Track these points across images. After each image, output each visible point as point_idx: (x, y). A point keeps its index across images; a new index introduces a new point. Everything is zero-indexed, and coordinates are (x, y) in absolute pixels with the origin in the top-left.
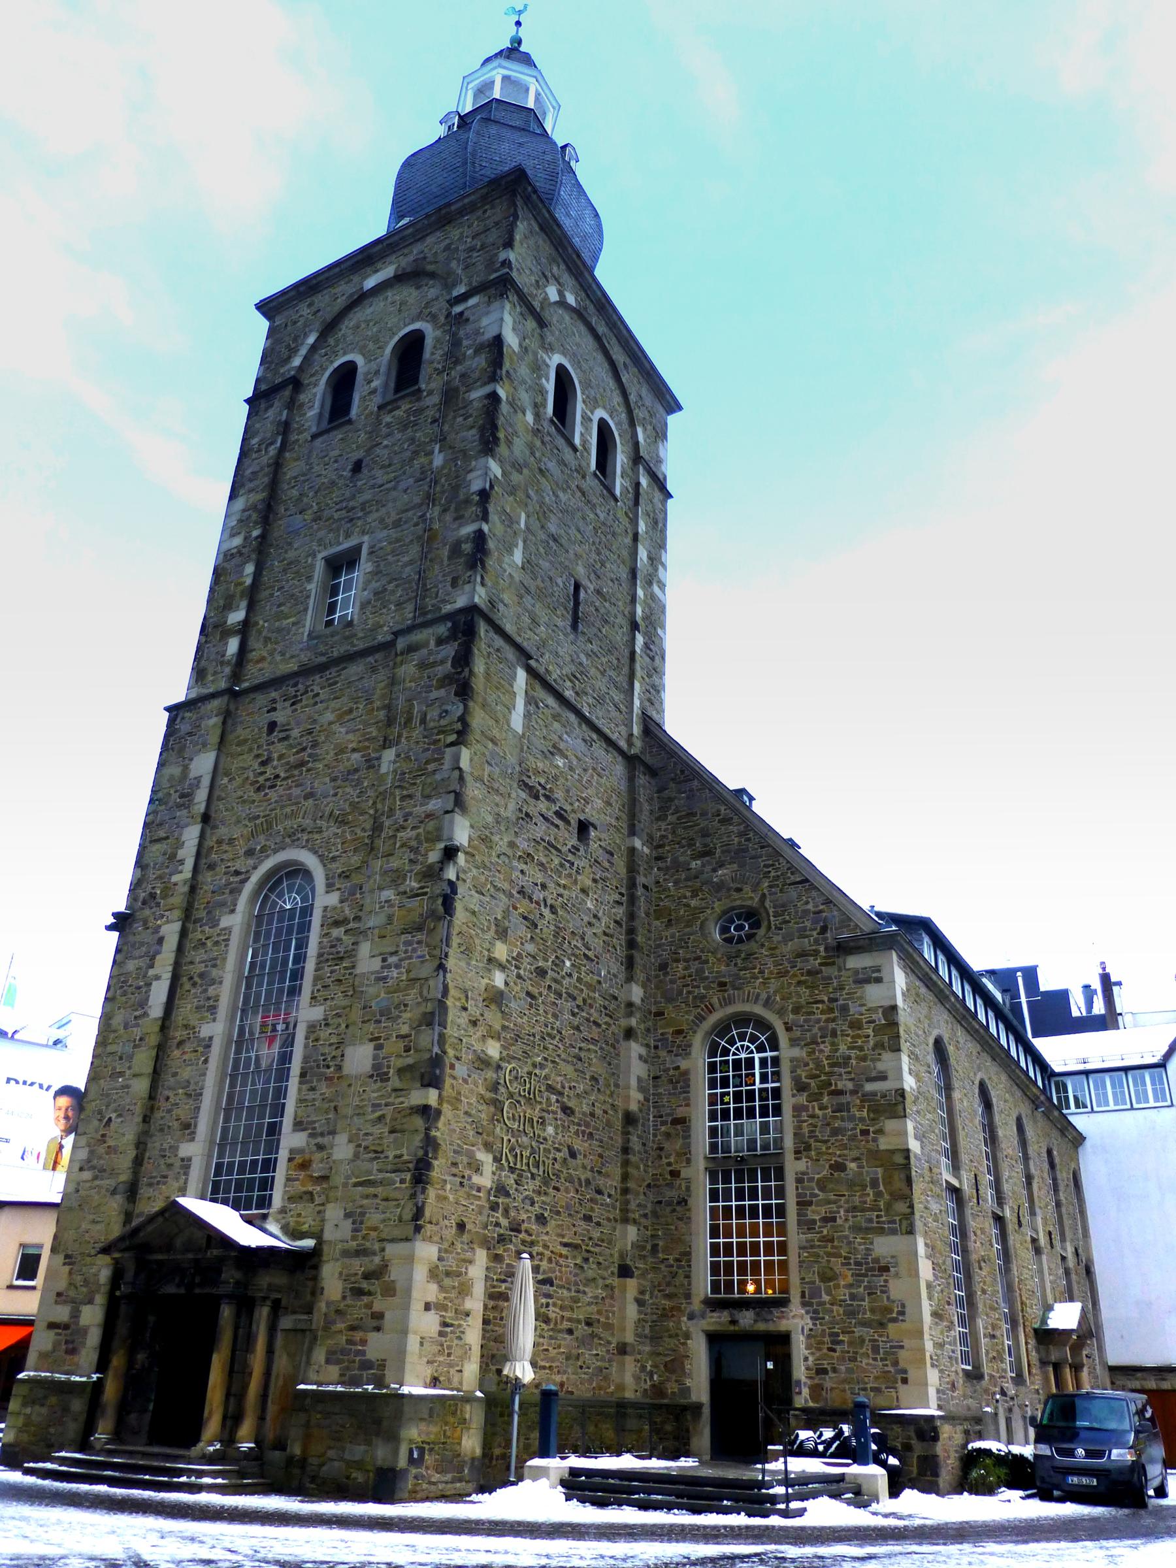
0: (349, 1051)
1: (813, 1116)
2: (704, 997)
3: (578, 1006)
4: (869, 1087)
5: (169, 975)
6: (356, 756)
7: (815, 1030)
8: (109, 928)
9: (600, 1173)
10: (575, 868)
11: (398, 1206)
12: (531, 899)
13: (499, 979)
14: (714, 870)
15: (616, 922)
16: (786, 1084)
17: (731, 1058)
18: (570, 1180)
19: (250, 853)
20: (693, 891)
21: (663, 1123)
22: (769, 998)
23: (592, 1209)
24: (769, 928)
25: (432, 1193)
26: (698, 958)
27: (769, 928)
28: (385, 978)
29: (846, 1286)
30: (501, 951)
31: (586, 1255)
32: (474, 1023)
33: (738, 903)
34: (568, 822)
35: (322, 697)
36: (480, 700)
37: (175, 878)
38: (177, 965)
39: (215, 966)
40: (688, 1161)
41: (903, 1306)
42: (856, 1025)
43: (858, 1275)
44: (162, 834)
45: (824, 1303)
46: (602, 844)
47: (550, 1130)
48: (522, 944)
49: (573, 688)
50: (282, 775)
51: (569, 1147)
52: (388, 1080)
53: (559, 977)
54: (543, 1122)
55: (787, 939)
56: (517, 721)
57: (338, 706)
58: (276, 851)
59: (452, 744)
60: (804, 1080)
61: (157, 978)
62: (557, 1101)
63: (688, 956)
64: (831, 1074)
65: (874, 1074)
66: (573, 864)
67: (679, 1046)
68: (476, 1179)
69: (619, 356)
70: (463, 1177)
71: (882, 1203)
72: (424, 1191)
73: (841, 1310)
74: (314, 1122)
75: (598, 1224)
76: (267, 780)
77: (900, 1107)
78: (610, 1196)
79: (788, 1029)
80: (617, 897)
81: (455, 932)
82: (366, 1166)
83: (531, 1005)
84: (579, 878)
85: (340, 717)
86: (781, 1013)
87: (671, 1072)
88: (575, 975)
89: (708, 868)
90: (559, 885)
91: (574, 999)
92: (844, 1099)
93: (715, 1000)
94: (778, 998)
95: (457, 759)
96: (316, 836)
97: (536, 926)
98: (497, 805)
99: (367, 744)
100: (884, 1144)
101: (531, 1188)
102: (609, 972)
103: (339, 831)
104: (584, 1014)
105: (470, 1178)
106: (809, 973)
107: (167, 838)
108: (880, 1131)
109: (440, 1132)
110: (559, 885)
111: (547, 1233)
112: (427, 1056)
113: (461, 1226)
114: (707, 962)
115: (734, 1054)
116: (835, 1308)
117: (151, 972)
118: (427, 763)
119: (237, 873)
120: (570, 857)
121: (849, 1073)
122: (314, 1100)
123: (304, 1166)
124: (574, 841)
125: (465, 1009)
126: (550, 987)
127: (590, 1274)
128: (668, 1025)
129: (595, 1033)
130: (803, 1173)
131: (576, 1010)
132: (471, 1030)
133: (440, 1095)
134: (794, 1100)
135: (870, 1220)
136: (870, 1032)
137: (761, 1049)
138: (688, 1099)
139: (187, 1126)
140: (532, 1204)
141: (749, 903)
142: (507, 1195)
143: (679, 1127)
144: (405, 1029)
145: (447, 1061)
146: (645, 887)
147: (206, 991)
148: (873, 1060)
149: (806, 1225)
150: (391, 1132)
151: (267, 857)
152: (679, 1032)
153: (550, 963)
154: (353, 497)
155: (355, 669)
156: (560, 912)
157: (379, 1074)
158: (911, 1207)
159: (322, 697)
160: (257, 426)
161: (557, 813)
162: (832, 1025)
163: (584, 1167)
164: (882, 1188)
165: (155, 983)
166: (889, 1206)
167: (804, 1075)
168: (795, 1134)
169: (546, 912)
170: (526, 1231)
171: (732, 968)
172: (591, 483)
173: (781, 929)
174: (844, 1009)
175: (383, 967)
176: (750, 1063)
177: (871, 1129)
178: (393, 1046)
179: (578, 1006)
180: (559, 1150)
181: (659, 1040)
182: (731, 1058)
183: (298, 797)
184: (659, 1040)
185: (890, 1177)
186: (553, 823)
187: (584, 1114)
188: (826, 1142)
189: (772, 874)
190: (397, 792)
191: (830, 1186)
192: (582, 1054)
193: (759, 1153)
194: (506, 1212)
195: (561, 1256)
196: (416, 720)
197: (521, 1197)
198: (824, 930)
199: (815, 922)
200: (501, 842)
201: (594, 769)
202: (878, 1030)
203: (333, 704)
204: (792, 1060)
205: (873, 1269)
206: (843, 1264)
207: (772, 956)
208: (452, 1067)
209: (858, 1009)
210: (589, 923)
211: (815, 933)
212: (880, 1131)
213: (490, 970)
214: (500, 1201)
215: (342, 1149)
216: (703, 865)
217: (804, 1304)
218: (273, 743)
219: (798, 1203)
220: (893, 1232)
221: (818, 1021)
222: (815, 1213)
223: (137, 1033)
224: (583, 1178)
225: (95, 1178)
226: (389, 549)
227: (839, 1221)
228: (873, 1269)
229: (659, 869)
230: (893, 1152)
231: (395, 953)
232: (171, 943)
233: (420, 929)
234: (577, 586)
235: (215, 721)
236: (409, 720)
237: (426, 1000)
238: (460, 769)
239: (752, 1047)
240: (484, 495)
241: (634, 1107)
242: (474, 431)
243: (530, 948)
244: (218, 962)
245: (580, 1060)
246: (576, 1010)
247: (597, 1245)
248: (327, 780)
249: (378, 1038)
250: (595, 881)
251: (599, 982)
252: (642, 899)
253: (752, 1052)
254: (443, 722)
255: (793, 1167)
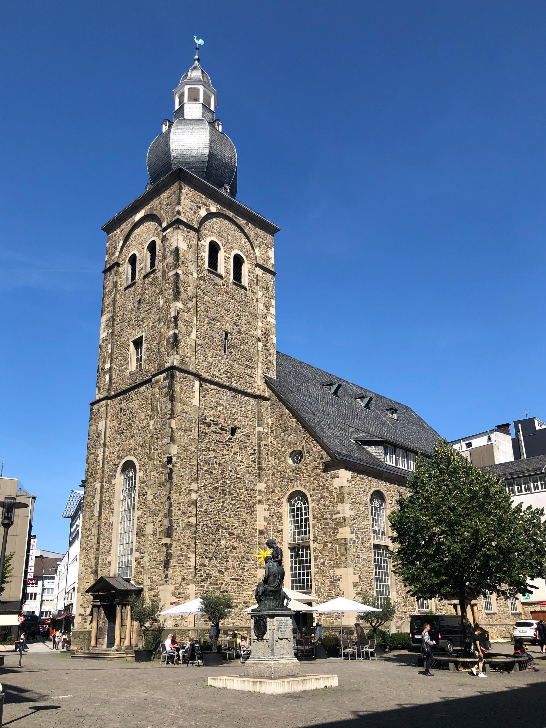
0: (146, 526)
1: (318, 528)
2: (286, 485)
3: (234, 497)
4: (335, 516)
5: (99, 502)
6: (145, 421)
7: (319, 496)
8: (80, 486)
9: (248, 553)
10: (230, 447)
11: (160, 575)
12: (209, 464)
13: (194, 496)
14: (288, 437)
15: (252, 461)
16: (311, 517)
17: (295, 507)
18: (234, 557)
19: (118, 457)
20: (282, 445)
21: (275, 532)
22: (305, 486)
23: (245, 566)
24: (305, 458)
25: (171, 571)
26: (284, 471)
27: (305, 458)
28: (155, 502)
29: (327, 586)
30: (194, 486)
31: (243, 581)
32: (184, 513)
33: (296, 449)
34: (226, 431)
35: (134, 399)
36: (178, 400)
37: (98, 467)
38: (101, 498)
39: (112, 498)
40: (283, 545)
41: (343, 592)
42: (331, 495)
43: (331, 582)
44: (93, 451)
45: (321, 592)
46: (244, 433)
47: (223, 542)
48: (206, 480)
49: (227, 377)
50: (125, 428)
51: (232, 546)
52: (156, 535)
53: (224, 488)
54: (219, 540)
55: (311, 462)
56: (196, 402)
57: (139, 403)
58: (125, 457)
59: (169, 419)
60: (316, 515)
61: (96, 503)
62: (226, 531)
63: (281, 470)
64: (323, 512)
65: (336, 512)
66: (229, 445)
67: (279, 504)
68: (188, 563)
69: (242, 221)
70: (183, 563)
71: (338, 558)
72: (167, 570)
73: (326, 594)
74: (141, 549)
75: (248, 570)
76: (121, 430)
77: (344, 523)
78: (253, 560)
79: (311, 496)
80: (252, 452)
81: (173, 485)
82: (152, 563)
83: (212, 501)
84: (232, 449)
85: (139, 407)
86: (309, 490)
87: (277, 514)
88: (232, 486)
89: (286, 436)
90: (223, 455)
91: (233, 494)
92: (327, 521)
93: (289, 486)
94: (308, 485)
95: (170, 424)
96: (136, 451)
97: (212, 473)
98: (189, 435)
99: (147, 417)
100: (339, 536)
101: (216, 562)
102: (249, 481)
103: (141, 449)
104: (238, 499)
105: (186, 563)
106: (317, 475)
107: (94, 453)
108: (338, 532)
109: (173, 550)
110: (223, 455)
111: (224, 576)
112: (166, 527)
113: (184, 579)
114: (287, 472)
115: (297, 506)
116: (325, 593)
117: (94, 501)
118: (162, 426)
119: (115, 465)
120: (228, 443)
121: (329, 512)
122: (140, 542)
123: (139, 563)
124: (230, 436)
125: (180, 509)
126: (220, 493)
127: (245, 587)
128: (276, 496)
129: (243, 504)
130: (315, 548)
131: (234, 498)
132: (183, 516)
133: (171, 539)
134: (313, 522)
135: (335, 564)
136: (335, 496)
137: (304, 504)
138: (282, 523)
139: (108, 552)
140: (216, 567)
141: (299, 449)
142: (206, 566)
143: (279, 533)
144: (160, 519)
145: (174, 528)
146: (265, 445)
147: (110, 506)
148: (336, 507)
149: (317, 566)
150: (158, 552)
151: (123, 459)
152: (279, 499)
153: (220, 484)
154: (139, 316)
155: (143, 388)
156: (223, 464)
157: (155, 534)
158: (346, 558)
159: (134, 399)
160: (107, 283)
161: (221, 429)
162: (324, 494)
163: (241, 552)
164: (338, 552)
165: (96, 504)
166: (340, 558)
167: (316, 513)
168: (313, 534)
169: (217, 467)
170: (214, 577)
171: (294, 474)
172: (231, 286)
173: (309, 459)
174: (328, 488)
175: (154, 498)
176: (301, 508)
177: (335, 532)
178: (157, 525)
179: (234, 497)
180: (228, 548)
181: (273, 502)
182: (295, 507)
183: (130, 436)
184: (273, 502)
185: (340, 548)
186: (218, 433)
187: (239, 534)
188: (322, 537)
189: (306, 437)
190: (155, 436)
191: (323, 552)
192: (237, 513)
193: (304, 541)
194: (205, 572)
195: (231, 583)
196: (159, 409)
197: (211, 566)
198: (321, 458)
199: (319, 455)
200: (193, 448)
201: (238, 406)
202: (338, 495)
203: (137, 401)
204: (312, 507)
205: (335, 580)
206: (327, 579)
207: (306, 469)
208: (176, 529)
209: (331, 488)
210: (239, 465)
211: (319, 460)
212: (338, 532)
213: (190, 494)
214: (202, 568)
215: (147, 558)
216: (285, 435)
217: (316, 593)
218: (122, 416)
219: (314, 559)
220: (341, 567)
221: (320, 492)
222: (319, 562)
223: (92, 521)
224: (240, 556)
225: (86, 569)
226: (150, 338)
227: (326, 564)
228: (335, 580)
229: (271, 437)
230: (341, 539)
231: (157, 493)
232: (99, 490)
233: (163, 485)
234: (226, 334)
235: (104, 408)
236: (157, 409)
237: (165, 509)
238: (171, 428)
239: (302, 503)
240: (176, 318)
241: (263, 528)
242: (171, 290)
243: (211, 481)
244: (112, 496)
245: (237, 515)
246: (234, 498)
247: (247, 577)
248: (137, 430)
249: (154, 522)
250: (240, 448)
251: (245, 486)
252: (264, 450)
253: (302, 505)
254: (166, 411)
255: (313, 545)
